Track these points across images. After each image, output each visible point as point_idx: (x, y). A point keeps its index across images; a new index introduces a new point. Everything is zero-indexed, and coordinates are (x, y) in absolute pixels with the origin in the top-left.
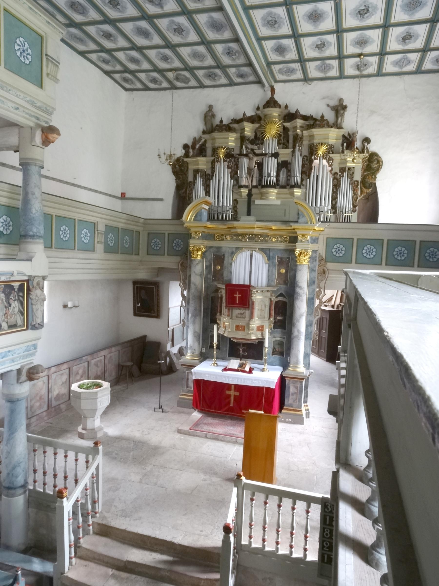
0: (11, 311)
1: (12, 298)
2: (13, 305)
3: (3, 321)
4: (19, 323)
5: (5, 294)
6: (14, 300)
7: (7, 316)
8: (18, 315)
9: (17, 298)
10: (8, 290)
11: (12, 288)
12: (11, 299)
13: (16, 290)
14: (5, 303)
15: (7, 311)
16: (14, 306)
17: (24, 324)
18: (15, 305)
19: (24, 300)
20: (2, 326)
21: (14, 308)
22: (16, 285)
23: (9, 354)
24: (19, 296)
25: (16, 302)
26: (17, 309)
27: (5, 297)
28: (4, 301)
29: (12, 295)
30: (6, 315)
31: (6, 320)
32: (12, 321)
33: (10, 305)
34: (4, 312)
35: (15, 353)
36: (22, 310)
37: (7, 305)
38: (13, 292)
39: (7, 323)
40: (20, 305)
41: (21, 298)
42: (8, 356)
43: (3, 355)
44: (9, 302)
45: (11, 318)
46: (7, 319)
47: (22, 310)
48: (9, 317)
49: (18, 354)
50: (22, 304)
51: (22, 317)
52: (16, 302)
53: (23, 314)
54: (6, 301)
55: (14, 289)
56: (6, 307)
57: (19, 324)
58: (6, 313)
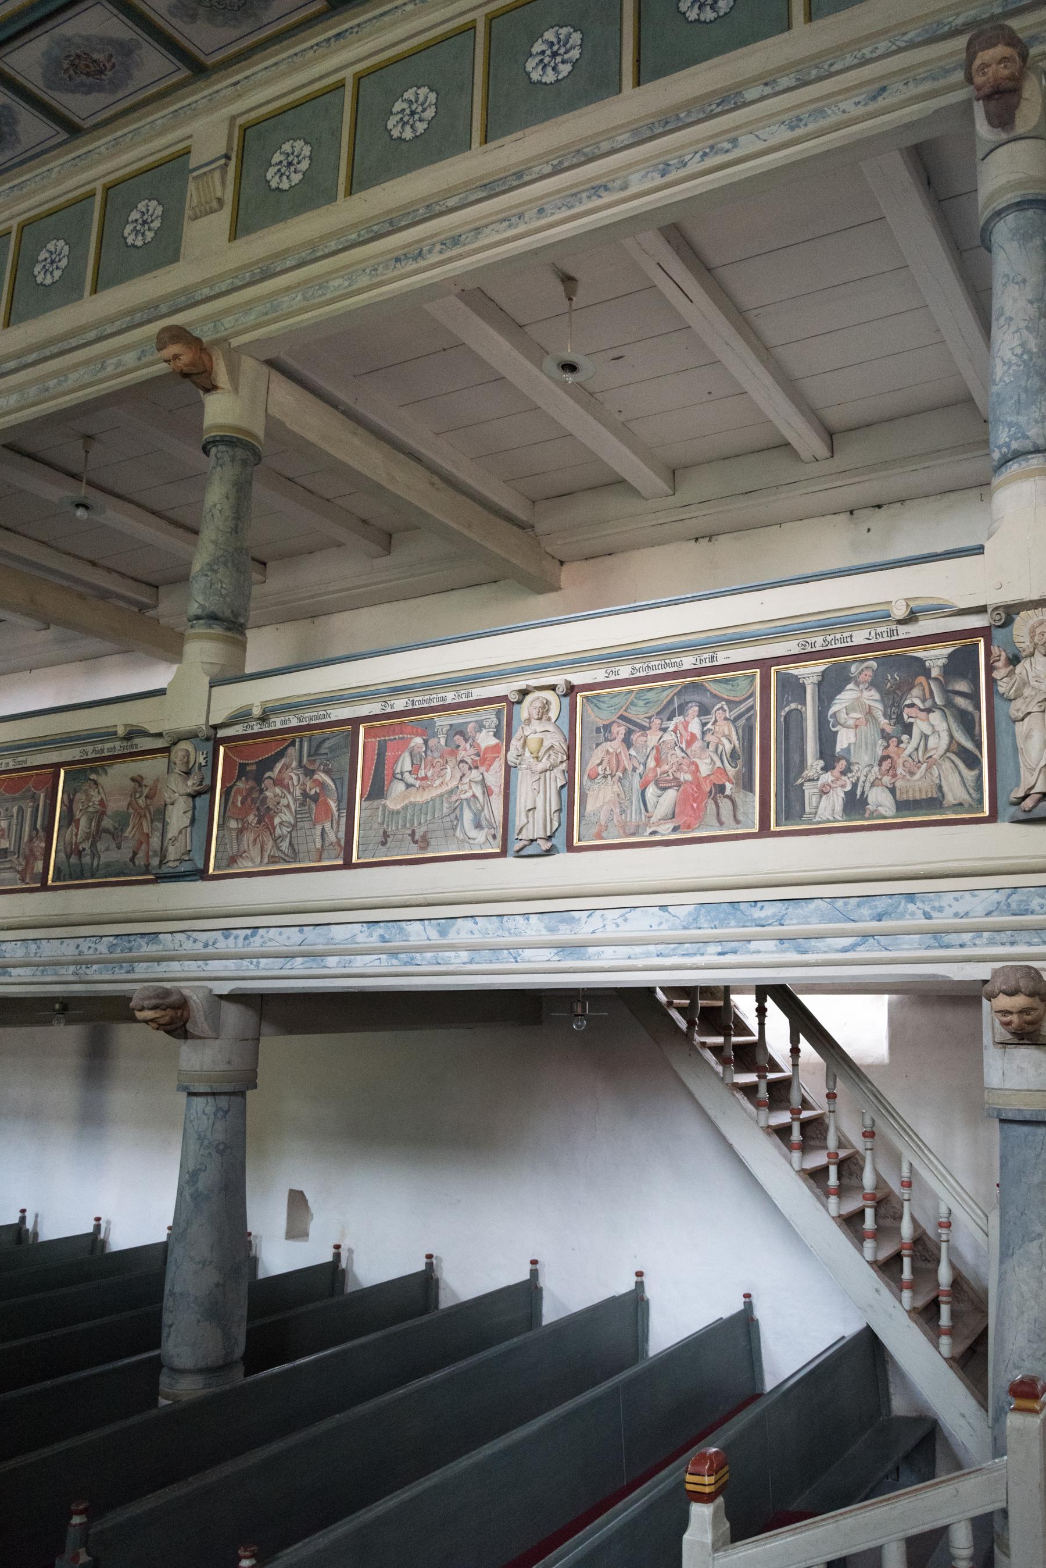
0: (910, 748)
1: (917, 702)
2: (920, 726)
3: (873, 785)
4: (955, 791)
5: (879, 690)
6: (929, 711)
7: (893, 767)
8: (947, 765)
9: (939, 700)
10: (894, 677)
11: (921, 668)
12: (913, 705)
13: (935, 673)
14: (883, 722)
15: (892, 749)
16: (928, 731)
17: (981, 801)
18: (935, 729)
19: (978, 707)
20: (870, 800)
21: (925, 737)
22: (936, 656)
23: (911, 907)
24: (949, 694)
25: (936, 717)
26: (939, 743)
27: (882, 700)
28: (879, 714)
29: (916, 692)
30: (886, 765)
31: (887, 780)
32: (917, 785)
33: (908, 729)
34: (880, 752)
35: (941, 909)
36: (969, 745)
37: (889, 729)
38: (921, 679)
39: (892, 791)
40: (954, 726)
41: (961, 702)
42: (902, 916)
43: (881, 904)
44: (900, 716)
45: (912, 774)
46: (894, 776)
47: (969, 745)
48: (900, 770)
49: (956, 915)
50: (968, 722)
51: (969, 775)
52: (936, 717)
53: (972, 761)
54: (885, 715)
55: (927, 672)
56: (886, 736)
57: (950, 799)
58: (884, 758)
